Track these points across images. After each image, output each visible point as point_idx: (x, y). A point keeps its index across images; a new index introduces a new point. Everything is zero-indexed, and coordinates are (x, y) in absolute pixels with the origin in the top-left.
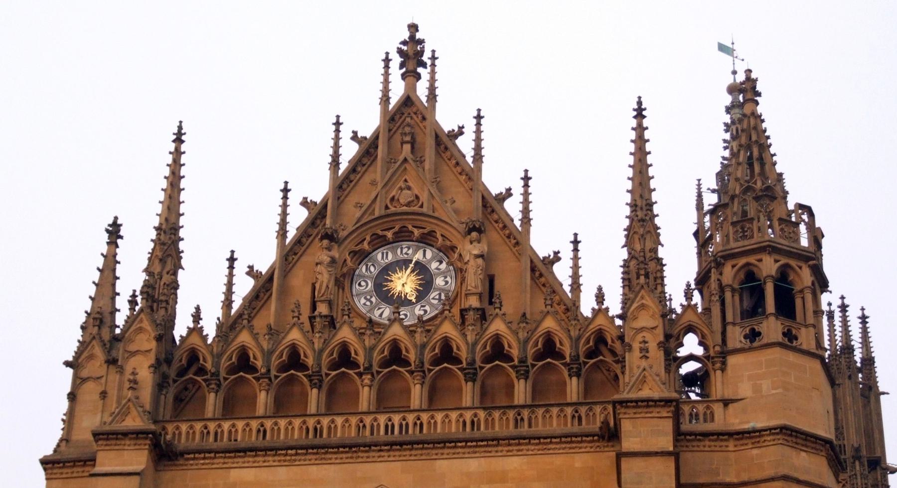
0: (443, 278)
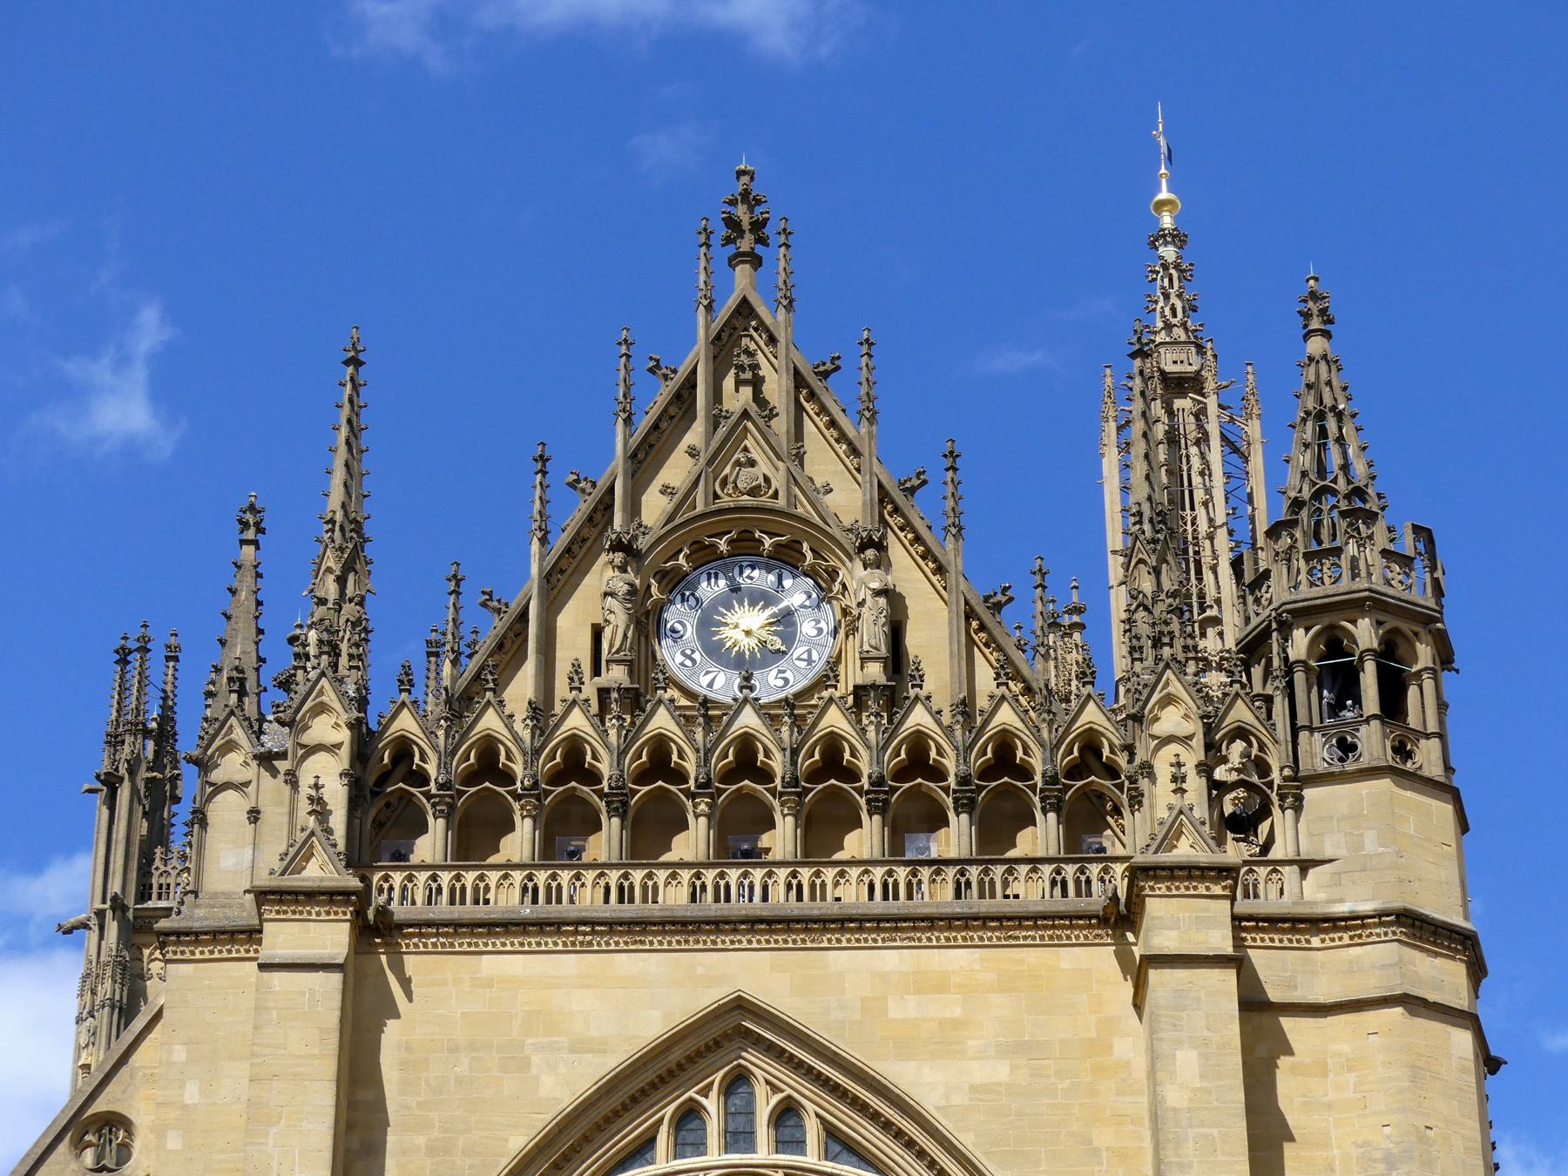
0: (814, 623)
